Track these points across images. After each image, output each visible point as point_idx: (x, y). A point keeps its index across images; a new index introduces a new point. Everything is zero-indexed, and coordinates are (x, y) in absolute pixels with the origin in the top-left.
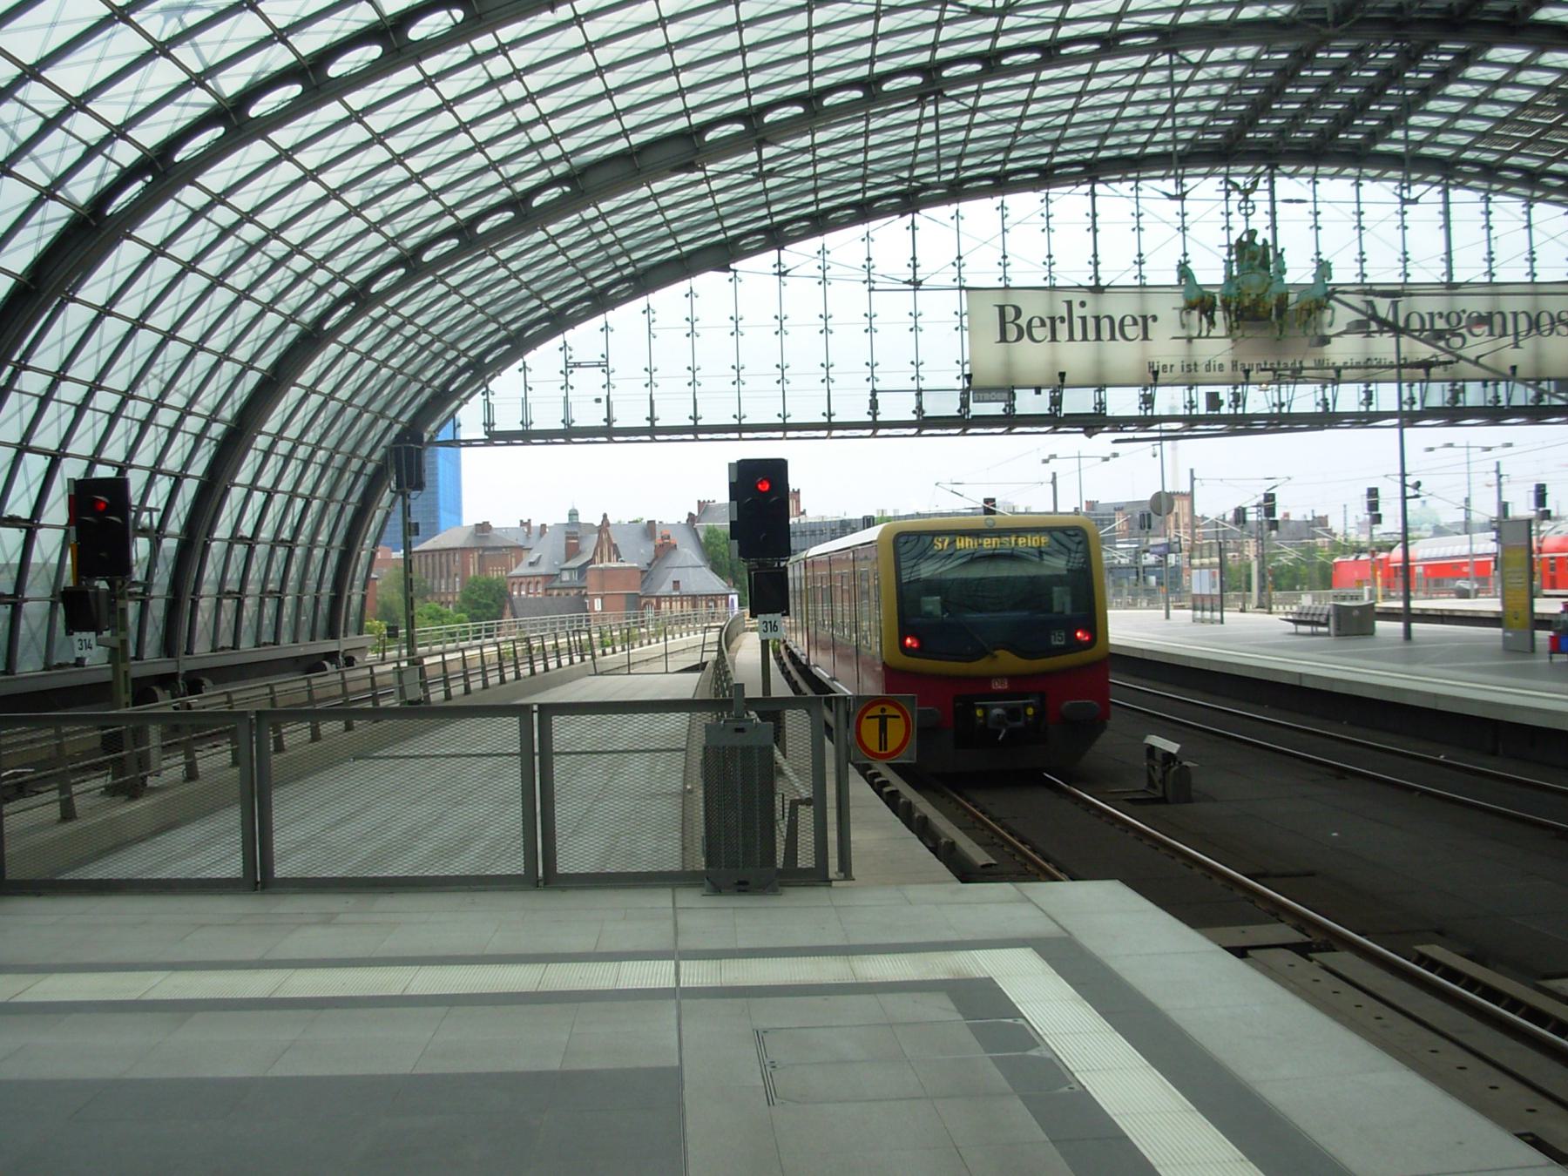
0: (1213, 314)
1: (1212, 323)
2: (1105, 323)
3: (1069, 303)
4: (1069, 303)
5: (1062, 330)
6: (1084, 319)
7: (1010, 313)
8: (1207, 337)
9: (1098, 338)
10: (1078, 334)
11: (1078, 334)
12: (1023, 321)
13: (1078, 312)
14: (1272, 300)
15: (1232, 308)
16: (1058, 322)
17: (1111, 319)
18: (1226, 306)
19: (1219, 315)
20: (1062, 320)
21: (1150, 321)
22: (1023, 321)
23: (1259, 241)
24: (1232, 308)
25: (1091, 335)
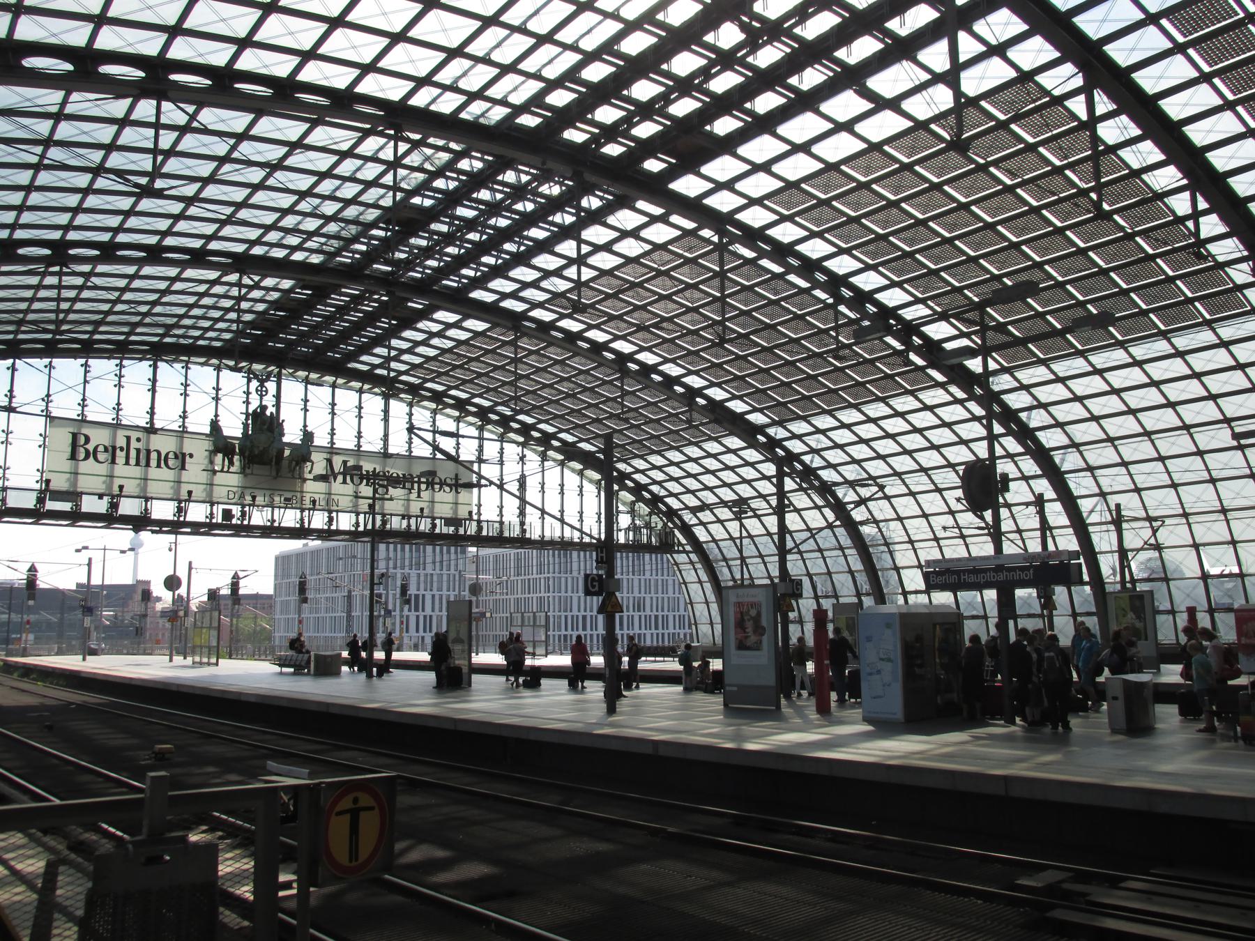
0: (233, 457)
1: (231, 463)
2: (154, 456)
3: (128, 438)
4: (128, 438)
5: (121, 457)
6: (138, 451)
7: (82, 440)
8: (228, 472)
9: (148, 465)
10: (132, 461)
11: (132, 461)
12: (91, 447)
13: (134, 444)
14: (274, 452)
15: (247, 454)
16: (118, 451)
17: (159, 453)
18: (242, 453)
19: (236, 458)
20: (122, 449)
21: (187, 457)
22: (91, 447)
23: (268, 413)
24: (247, 454)
25: (143, 462)
